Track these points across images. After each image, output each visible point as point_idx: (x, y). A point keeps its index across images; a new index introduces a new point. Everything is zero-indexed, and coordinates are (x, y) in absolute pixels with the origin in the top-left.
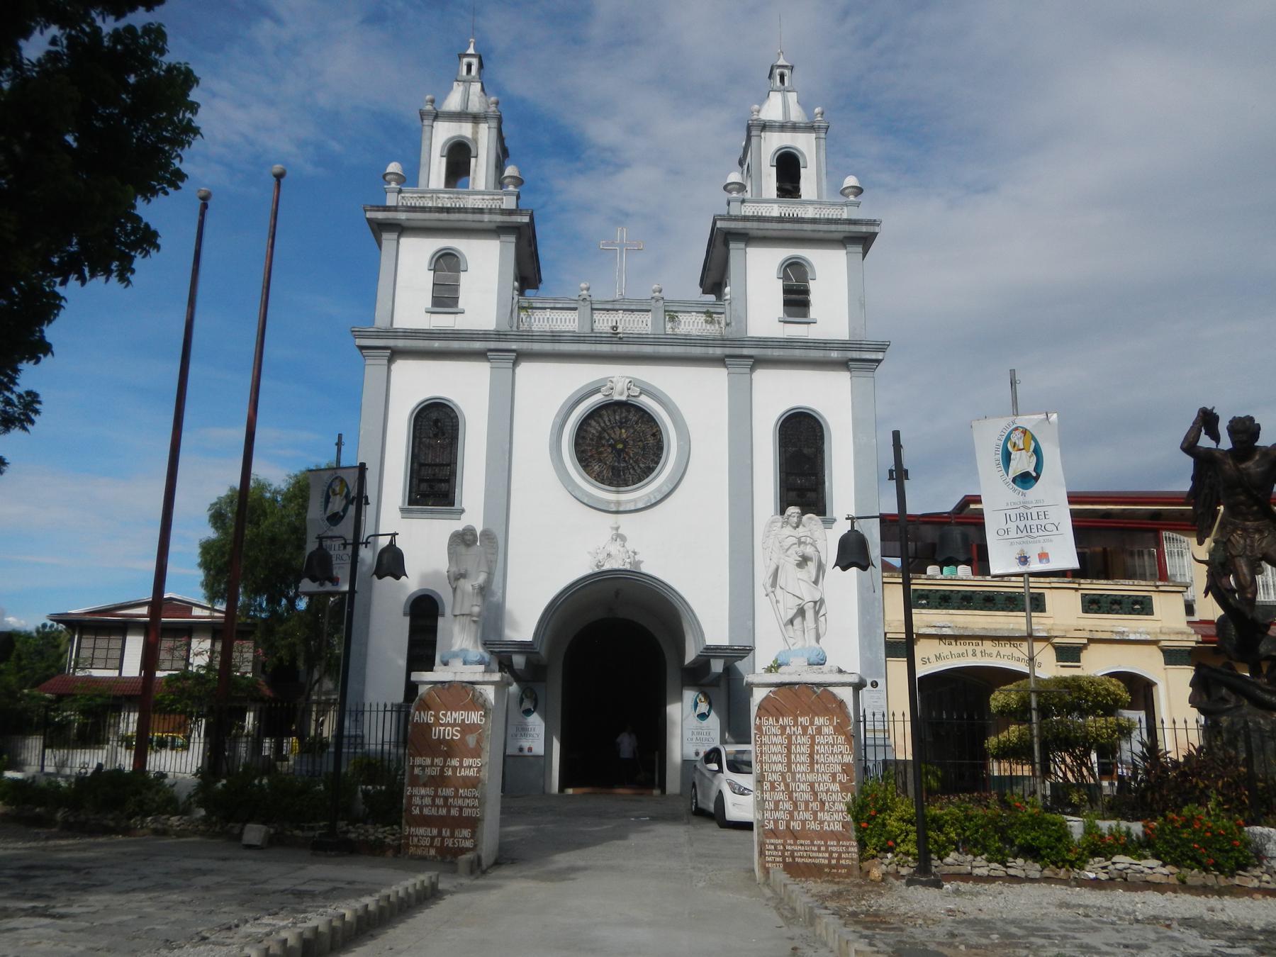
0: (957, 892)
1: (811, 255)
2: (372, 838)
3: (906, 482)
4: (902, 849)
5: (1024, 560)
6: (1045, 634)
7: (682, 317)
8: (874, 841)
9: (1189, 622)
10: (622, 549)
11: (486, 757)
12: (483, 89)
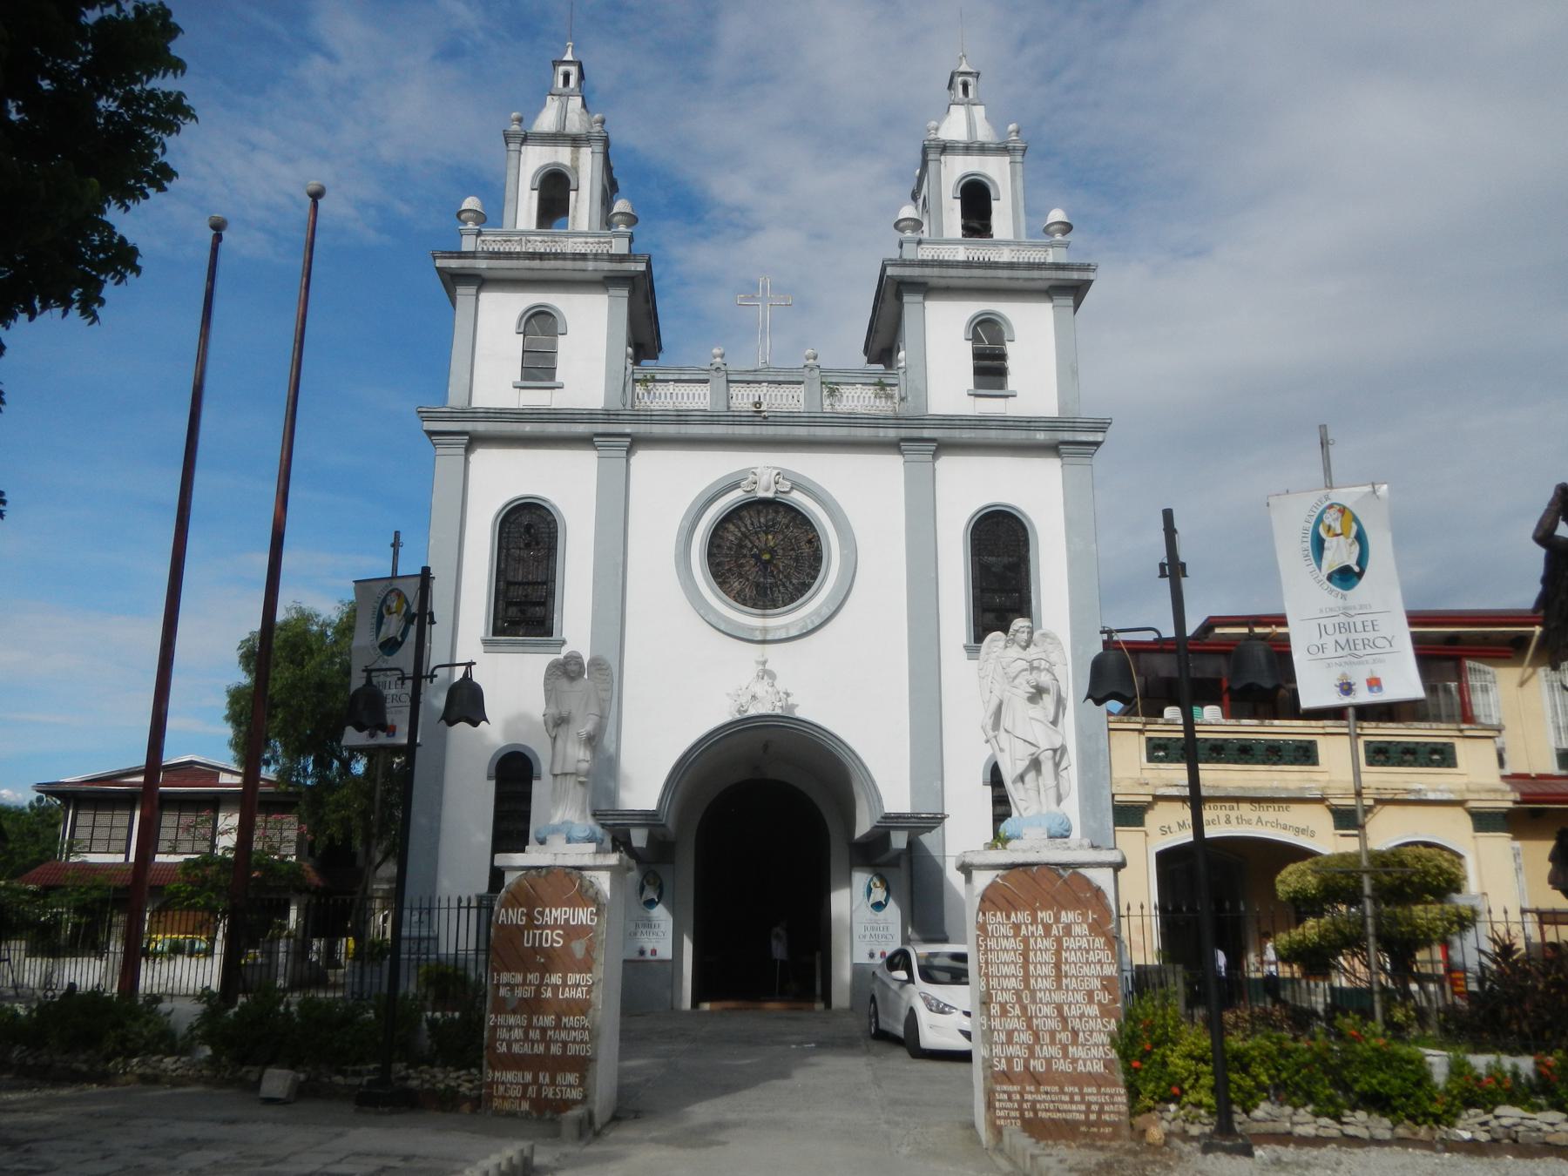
0: (1277, 1162)
1: (1011, 311)
2: (442, 1086)
3: (1184, 580)
4: (1191, 1099)
5: (1347, 688)
6: (1317, 794)
7: (843, 389)
8: (1151, 1086)
9: (1504, 777)
10: (770, 689)
11: (599, 972)
12: (584, 105)
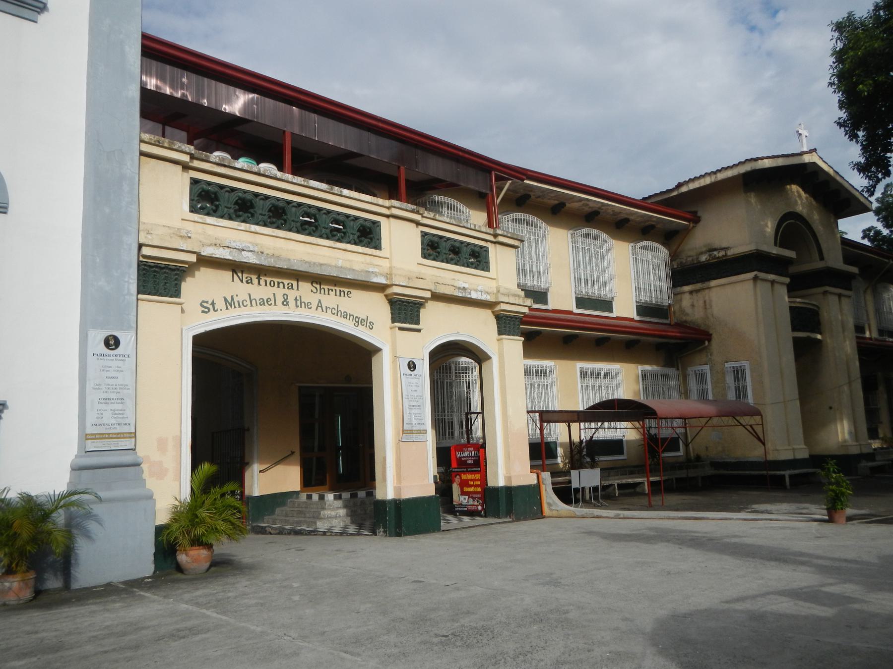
6: (382, 280)
